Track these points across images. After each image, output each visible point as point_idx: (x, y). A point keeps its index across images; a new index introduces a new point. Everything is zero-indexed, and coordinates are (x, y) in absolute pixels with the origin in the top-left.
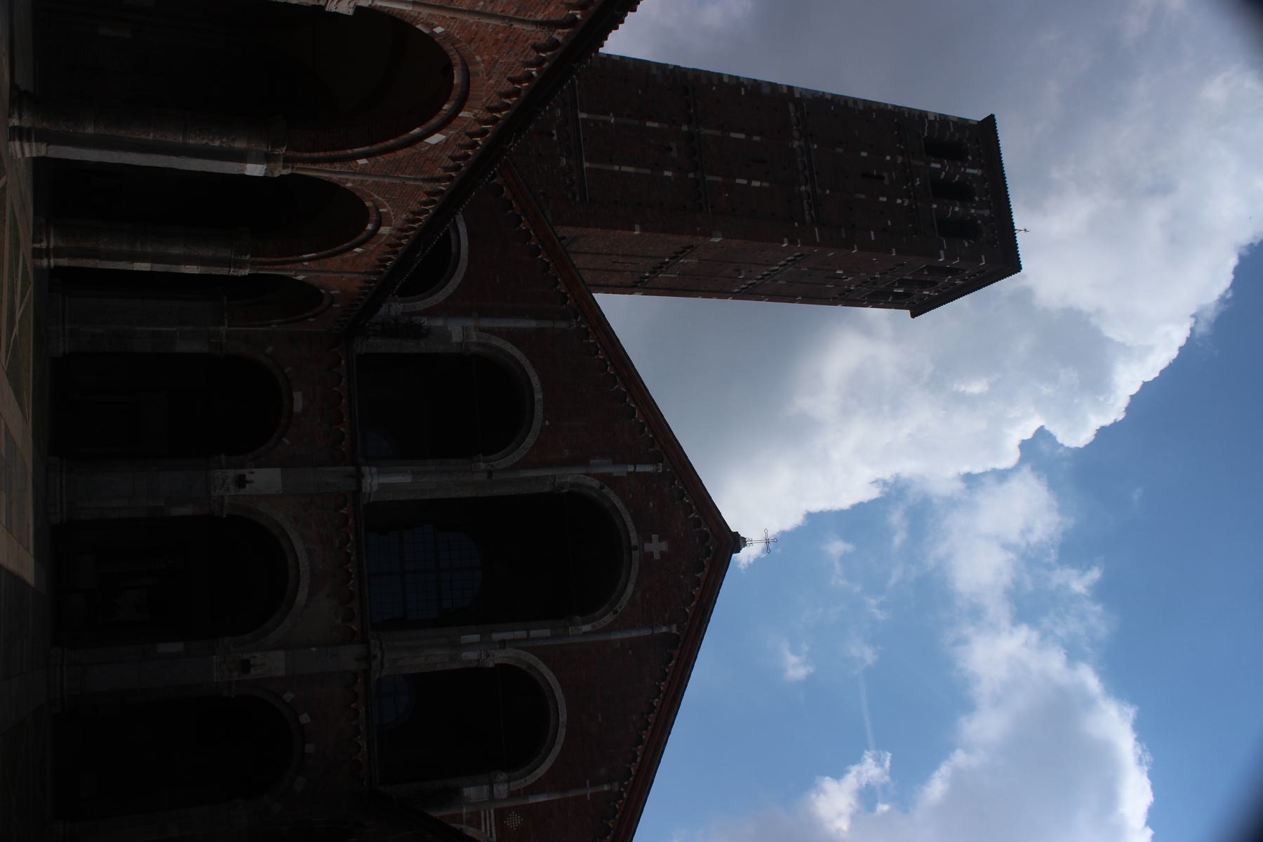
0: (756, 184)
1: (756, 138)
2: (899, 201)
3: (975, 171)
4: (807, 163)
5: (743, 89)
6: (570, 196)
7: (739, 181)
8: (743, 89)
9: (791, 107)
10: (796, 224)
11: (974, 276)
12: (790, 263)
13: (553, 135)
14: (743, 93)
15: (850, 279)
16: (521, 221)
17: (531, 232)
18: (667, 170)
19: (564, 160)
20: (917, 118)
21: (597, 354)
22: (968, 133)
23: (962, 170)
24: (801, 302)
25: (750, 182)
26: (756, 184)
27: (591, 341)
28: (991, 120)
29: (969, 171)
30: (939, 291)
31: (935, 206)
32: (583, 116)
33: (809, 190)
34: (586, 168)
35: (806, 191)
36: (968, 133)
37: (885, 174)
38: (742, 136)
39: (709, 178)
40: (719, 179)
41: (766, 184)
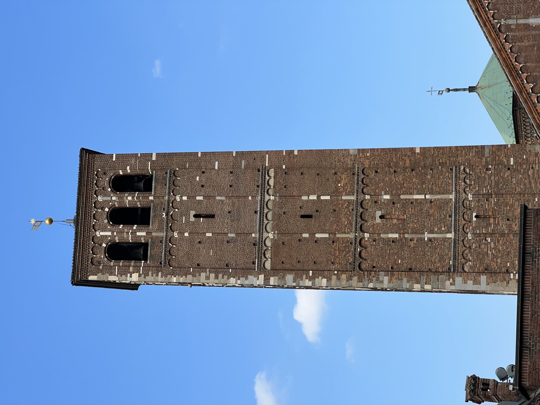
0: (313, 197)
1: (306, 235)
2: (185, 198)
3: (102, 233)
4: (265, 219)
5: (311, 275)
6: (468, 170)
7: (328, 198)
8: (311, 275)
9: (268, 265)
10: (284, 167)
13: (475, 217)
14: (311, 272)
16: (532, 89)
17: (526, 82)
19: (470, 197)
20: (150, 273)
21: (489, 3)
25: (319, 197)
26: (313, 197)
27: (492, 11)
29: (109, 234)
31: (151, 198)
32: (450, 236)
34: (451, 194)
35: (269, 195)
36: (101, 267)
37: (192, 219)
38: (317, 235)
39: (353, 198)
40: (344, 198)
41: (304, 198)
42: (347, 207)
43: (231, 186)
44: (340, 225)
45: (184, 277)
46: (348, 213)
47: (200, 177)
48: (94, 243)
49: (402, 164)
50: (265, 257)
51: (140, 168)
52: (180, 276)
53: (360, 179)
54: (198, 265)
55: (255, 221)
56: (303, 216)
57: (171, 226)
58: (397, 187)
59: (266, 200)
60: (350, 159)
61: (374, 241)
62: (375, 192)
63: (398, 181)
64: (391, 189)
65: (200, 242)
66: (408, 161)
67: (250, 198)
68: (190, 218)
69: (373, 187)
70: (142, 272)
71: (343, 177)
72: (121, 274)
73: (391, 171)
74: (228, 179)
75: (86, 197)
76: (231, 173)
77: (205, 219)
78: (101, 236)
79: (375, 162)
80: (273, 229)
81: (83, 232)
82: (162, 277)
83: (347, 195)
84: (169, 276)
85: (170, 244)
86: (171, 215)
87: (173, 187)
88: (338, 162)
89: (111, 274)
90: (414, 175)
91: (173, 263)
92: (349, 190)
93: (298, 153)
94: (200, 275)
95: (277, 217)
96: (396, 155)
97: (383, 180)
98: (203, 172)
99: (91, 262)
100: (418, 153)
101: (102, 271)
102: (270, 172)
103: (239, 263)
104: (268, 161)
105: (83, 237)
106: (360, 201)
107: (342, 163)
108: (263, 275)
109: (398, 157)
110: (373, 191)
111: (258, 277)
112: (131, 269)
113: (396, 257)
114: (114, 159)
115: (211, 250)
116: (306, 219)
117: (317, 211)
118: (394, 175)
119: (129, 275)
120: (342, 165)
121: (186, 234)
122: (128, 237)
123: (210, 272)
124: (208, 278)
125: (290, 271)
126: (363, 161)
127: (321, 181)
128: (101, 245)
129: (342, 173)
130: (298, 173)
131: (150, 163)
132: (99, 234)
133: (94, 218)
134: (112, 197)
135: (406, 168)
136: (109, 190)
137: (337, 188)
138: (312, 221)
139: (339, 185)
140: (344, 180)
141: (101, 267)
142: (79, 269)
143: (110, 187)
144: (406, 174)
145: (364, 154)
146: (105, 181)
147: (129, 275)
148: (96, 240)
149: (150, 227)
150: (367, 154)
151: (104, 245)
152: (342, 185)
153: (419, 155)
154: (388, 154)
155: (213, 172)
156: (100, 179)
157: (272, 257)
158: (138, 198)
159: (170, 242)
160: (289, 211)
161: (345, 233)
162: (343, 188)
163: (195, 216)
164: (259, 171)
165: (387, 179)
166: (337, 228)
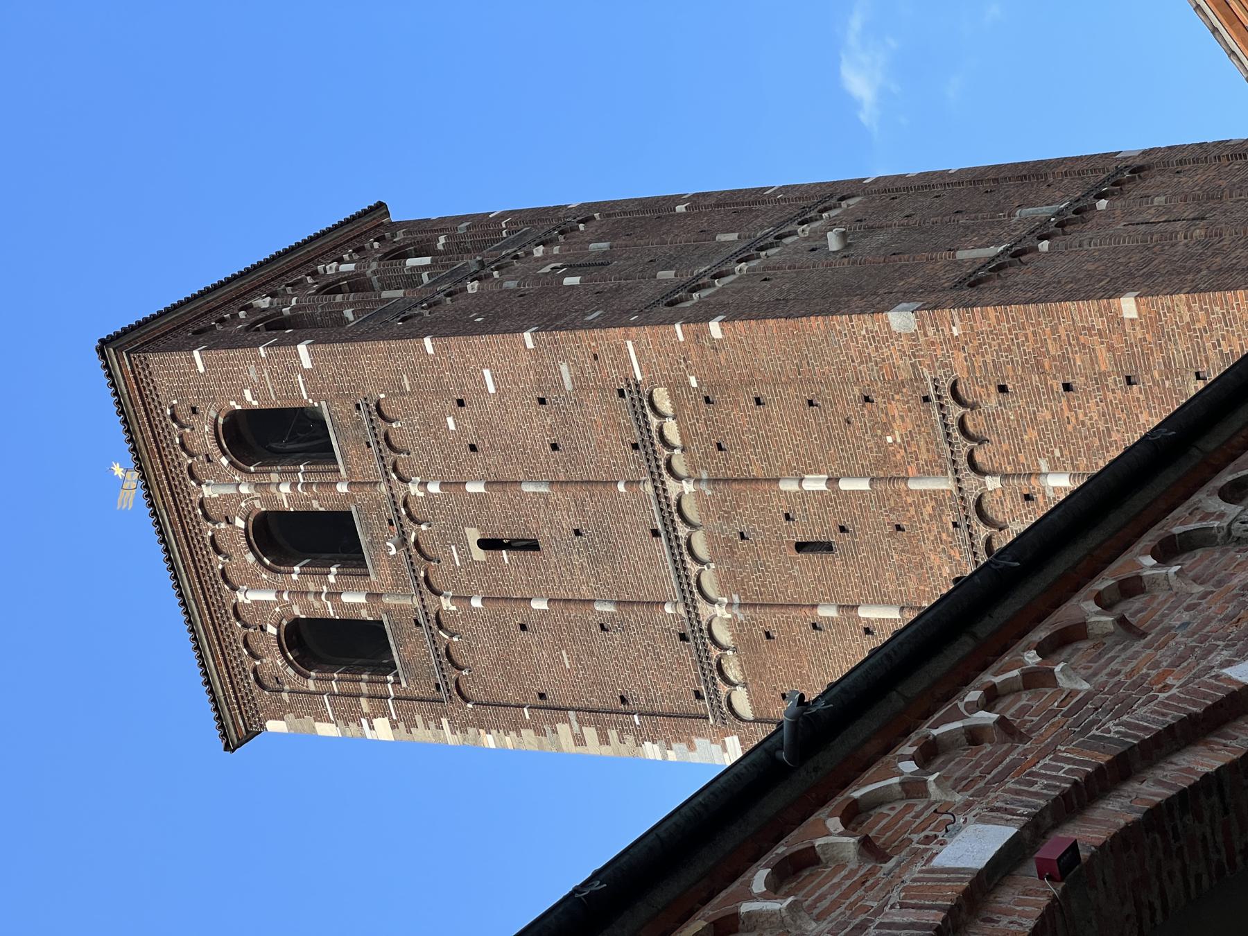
0: (815, 484)
3: (253, 596)
7: (863, 485)
10: (693, 382)
11: (222, 321)
12: (706, 280)
15: (547, 269)
20: (418, 718)
24: (677, 199)
25: (833, 481)
26: (815, 484)
29: (270, 596)
30: (314, 274)
33: (671, 484)
35: (678, 478)
37: (479, 555)
39: (945, 484)
40: (913, 485)
42: (937, 516)
43: (555, 447)
44: (929, 578)
45: (513, 734)
46: (944, 536)
47: (456, 418)
48: (245, 626)
49: (1083, 361)
50: (727, 681)
51: (279, 394)
52: (501, 731)
53: (953, 420)
54: (542, 696)
55: (662, 561)
56: (800, 547)
57: (426, 579)
58: (1087, 444)
59: (673, 498)
60: (900, 350)
62: (1016, 462)
63: (1088, 423)
64: (1070, 453)
65: (523, 627)
66: (1102, 351)
67: (621, 487)
68: (470, 550)
69: (1005, 447)
70: (397, 716)
71: (895, 409)
73: (1051, 385)
74: (540, 426)
75: (171, 489)
76: (542, 401)
77: (514, 555)
78: (255, 602)
79: (989, 358)
81: (204, 593)
83: (924, 474)
84: (471, 731)
85: (440, 632)
86: (417, 543)
87: (390, 457)
88: (862, 363)
89: (321, 717)
90: (1138, 399)
91: (471, 690)
92: (924, 456)
93: (723, 333)
94: (555, 731)
95: (725, 549)
96: (1054, 330)
97: (1031, 419)
99: (257, 680)
100: (1132, 320)
102: (656, 398)
103: (655, 694)
104: (640, 365)
105: (209, 608)
106: (972, 499)
107: (876, 365)
108: (736, 738)
109: (1064, 337)
110: (1008, 459)
111: (724, 742)
114: (201, 369)
115: (564, 652)
117: (843, 529)
118: (1068, 400)
119: (364, 721)
120: (878, 372)
121: (476, 603)
122: (325, 607)
123: (581, 723)
124: (580, 740)
126: (943, 355)
127: (828, 427)
128: (263, 629)
129: (889, 399)
130: (746, 401)
131: (299, 376)
133: (218, 551)
134: (238, 485)
135: (1105, 375)
137: (885, 456)
138: (834, 564)
140: (899, 421)
141: (285, 696)
142: (232, 704)
143: (224, 453)
144: (1110, 395)
145: (942, 330)
146: (203, 436)
147: (364, 721)
149: (373, 578)
150: (951, 330)
151: (272, 630)
152: (899, 440)
153: (1138, 328)
154: (1024, 329)
156: (188, 430)
157: (746, 678)
158: (307, 485)
160: (754, 530)
162: (906, 451)
165: (1047, 414)
166: (922, 588)
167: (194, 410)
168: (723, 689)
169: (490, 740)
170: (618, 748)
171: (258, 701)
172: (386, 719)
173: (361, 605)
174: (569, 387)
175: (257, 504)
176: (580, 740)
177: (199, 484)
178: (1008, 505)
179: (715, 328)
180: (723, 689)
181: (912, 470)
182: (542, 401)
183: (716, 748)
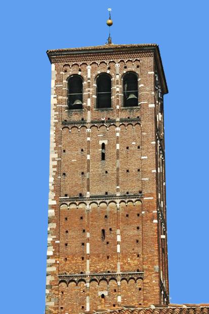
0: (119, 238)
5: (56, 242)
7: (119, 251)
9: (63, 207)
14: (58, 242)
18: (117, 300)
20: (57, 113)
22: (62, 73)
23: (89, 81)
25: (118, 243)
26: (119, 238)
28: (53, 56)
29: (89, 76)
33: (119, 200)
35: (120, 203)
36: (62, 73)
37: (101, 143)
39: (119, 272)
40: (119, 264)
45: (54, 140)
54: (64, 151)
56: (103, 231)
59: (115, 200)
61: (84, 291)
65: (82, 150)
67: (118, 187)
69: (127, 287)
71: (136, 262)
72: (57, 89)
74: (133, 169)
76: (139, 170)
80: (94, 209)
82: (54, 122)
83: (122, 267)
84: (55, 128)
89: (56, 81)
91: (66, 130)
94: (55, 153)
98: (139, 147)
99: (66, 65)
101: (59, 73)
112: (60, 97)
113: (70, 310)
116: (100, 233)
117: (108, 243)
119: (56, 96)
121: (89, 139)
123: (58, 161)
124: (54, 160)
125: (58, 225)
128: (80, 70)
132: (89, 67)
136: (125, 72)
139: (129, 259)
143: (127, 72)
146: (132, 68)
148: (83, 66)
155: (139, 156)
158: (118, 96)
159: (82, 126)
161: (90, 266)
163: (103, 144)
164: (140, 192)
165: (134, 299)
167: (138, 67)
168: (68, 203)
169: (52, 133)
170: (52, 171)
171: (60, 64)
172: (56, 103)
173: (87, 104)
174: (143, 179)
175: (113, 79)
176: (54, 160)
177: (119, 63)
178: (113, 285)
179: (155, 221)
180: (68, 203)
181: (122, 263)
182: (139, 170)
183: (53, 198)
